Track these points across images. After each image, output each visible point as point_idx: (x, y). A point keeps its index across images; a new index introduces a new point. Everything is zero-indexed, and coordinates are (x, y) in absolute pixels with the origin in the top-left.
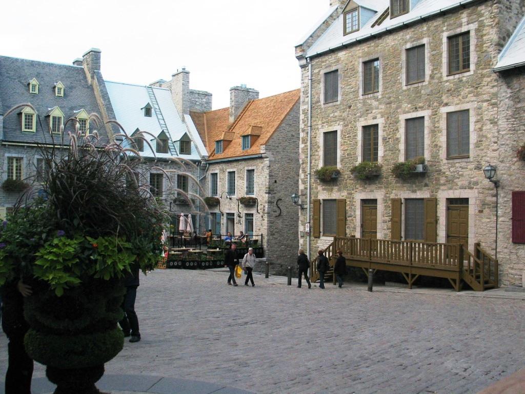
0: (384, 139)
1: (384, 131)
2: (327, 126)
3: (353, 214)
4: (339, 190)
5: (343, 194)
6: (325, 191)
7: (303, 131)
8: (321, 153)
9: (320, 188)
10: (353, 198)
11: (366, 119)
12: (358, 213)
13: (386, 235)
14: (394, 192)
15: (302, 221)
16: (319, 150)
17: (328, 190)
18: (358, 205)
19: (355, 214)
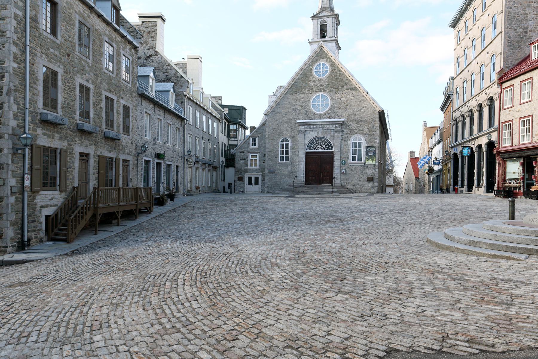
0: (94, 104)
1: (94, 96)
2: (46, 60)
3: (72, 165)
4: (61, 138)
5: (64, 144)
6: (46, 137)
7: (15, 44)
8: (41, 88)
9: (39, 131)
10: (73, 150)
11: (82, 78)
12: (77, 164)
13: (94, 184)
14: (100, 150)
15: (13, 171)
16: (37, 83)
17: (49, 136)
18: (77, 157)
19: (74, 166)
